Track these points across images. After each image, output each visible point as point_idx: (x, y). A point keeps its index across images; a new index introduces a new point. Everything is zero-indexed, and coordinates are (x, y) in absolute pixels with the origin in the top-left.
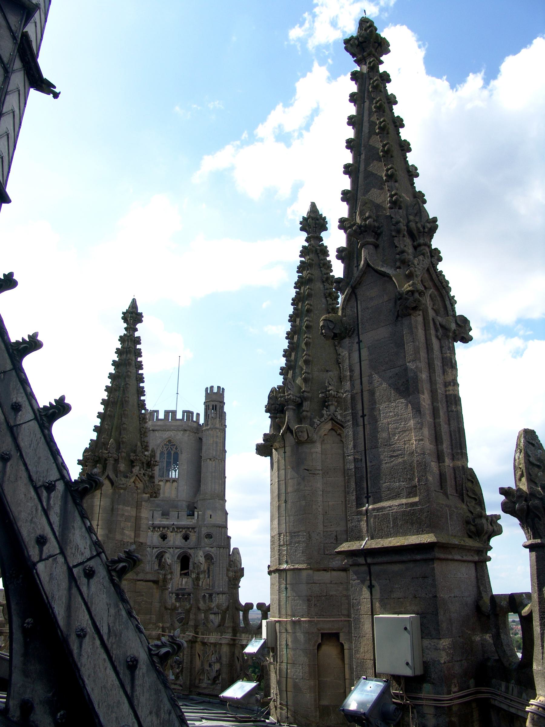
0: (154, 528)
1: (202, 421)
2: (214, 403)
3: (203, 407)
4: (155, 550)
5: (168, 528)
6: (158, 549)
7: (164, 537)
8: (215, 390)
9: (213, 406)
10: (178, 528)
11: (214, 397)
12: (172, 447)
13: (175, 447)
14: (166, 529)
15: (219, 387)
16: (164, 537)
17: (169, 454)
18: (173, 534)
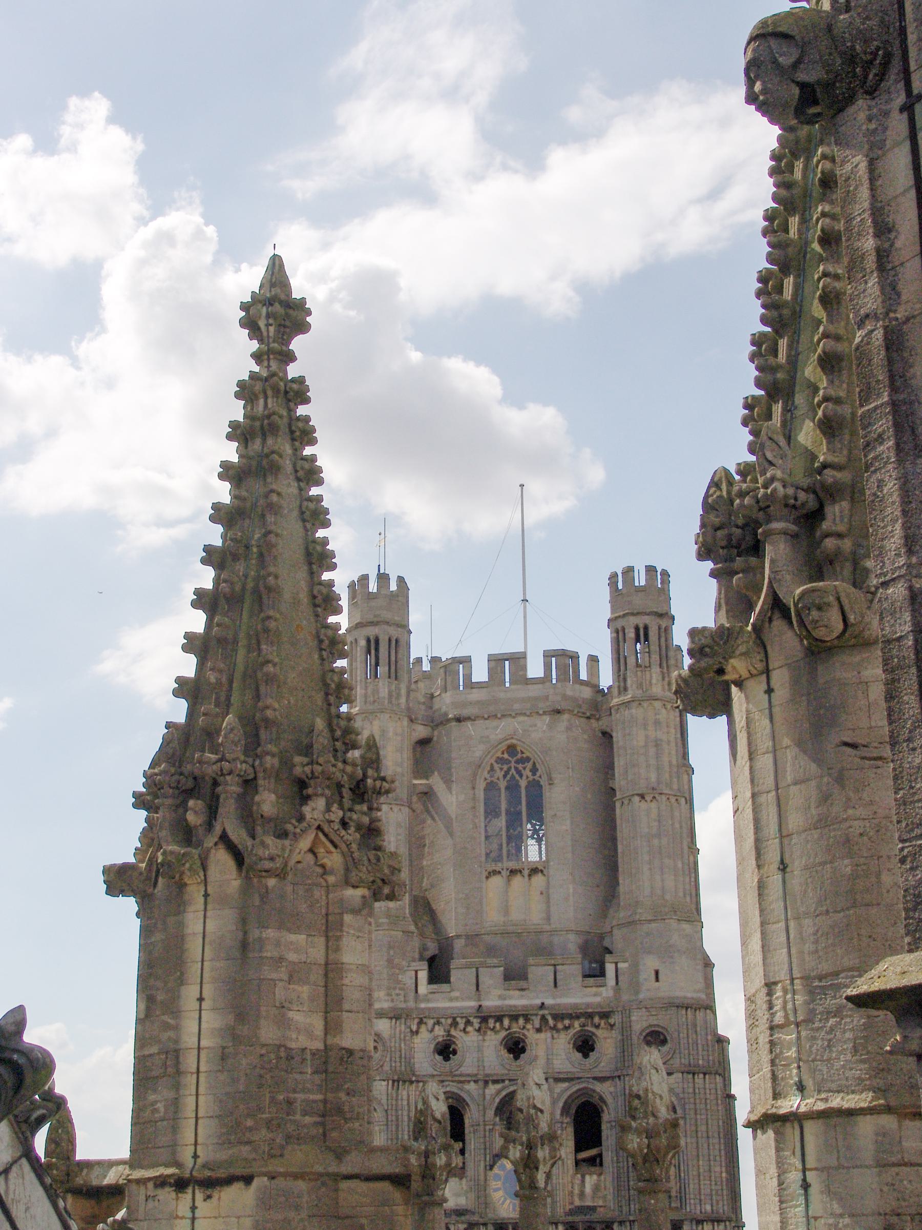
0: (484, 1020)
1: (606, 679)
3: (606, 636)
4: (492, 1089)
5: (527, 1019)
6: (499, 1086)
7: (516, 1048)
8: (641, 580)
9: (637, 629)
10: (557, 1017)
11: (638, 602)
12: (520, 766)
13: (529, 765)
14: (521, 1021)
15: (650, 570)
17: (513, 788)
18: (542, 1036)
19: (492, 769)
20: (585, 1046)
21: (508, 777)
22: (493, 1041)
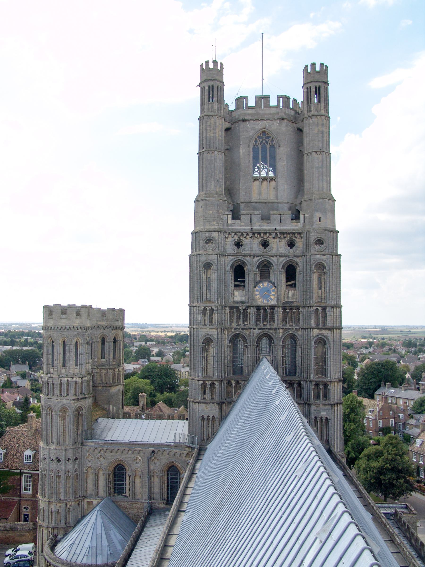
0: (254, 234)
2: (317, 84)
4: (256, 259)
5: (270, 234)
7: (265, 244)
8: (318, 68)
9: (316, 87)
10: (282, 233)
11: (317, 77)
12: (267, 140)
13: (271, 139)
14: (268, 235)
16: (265, 244)
17: (264, 148)
18: (275, 240)
19: (256, 141)
20: (291, 245)
21: (262, 144)
22: (257, 242)
